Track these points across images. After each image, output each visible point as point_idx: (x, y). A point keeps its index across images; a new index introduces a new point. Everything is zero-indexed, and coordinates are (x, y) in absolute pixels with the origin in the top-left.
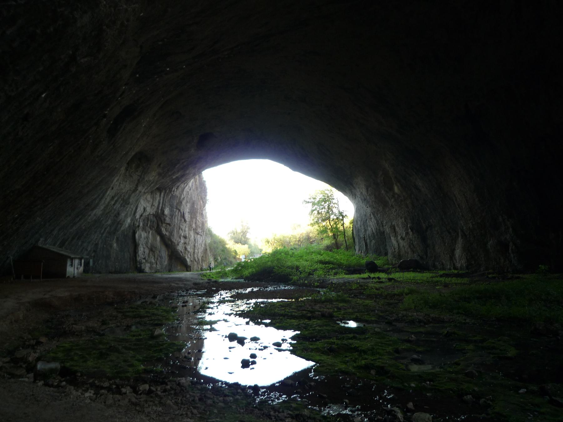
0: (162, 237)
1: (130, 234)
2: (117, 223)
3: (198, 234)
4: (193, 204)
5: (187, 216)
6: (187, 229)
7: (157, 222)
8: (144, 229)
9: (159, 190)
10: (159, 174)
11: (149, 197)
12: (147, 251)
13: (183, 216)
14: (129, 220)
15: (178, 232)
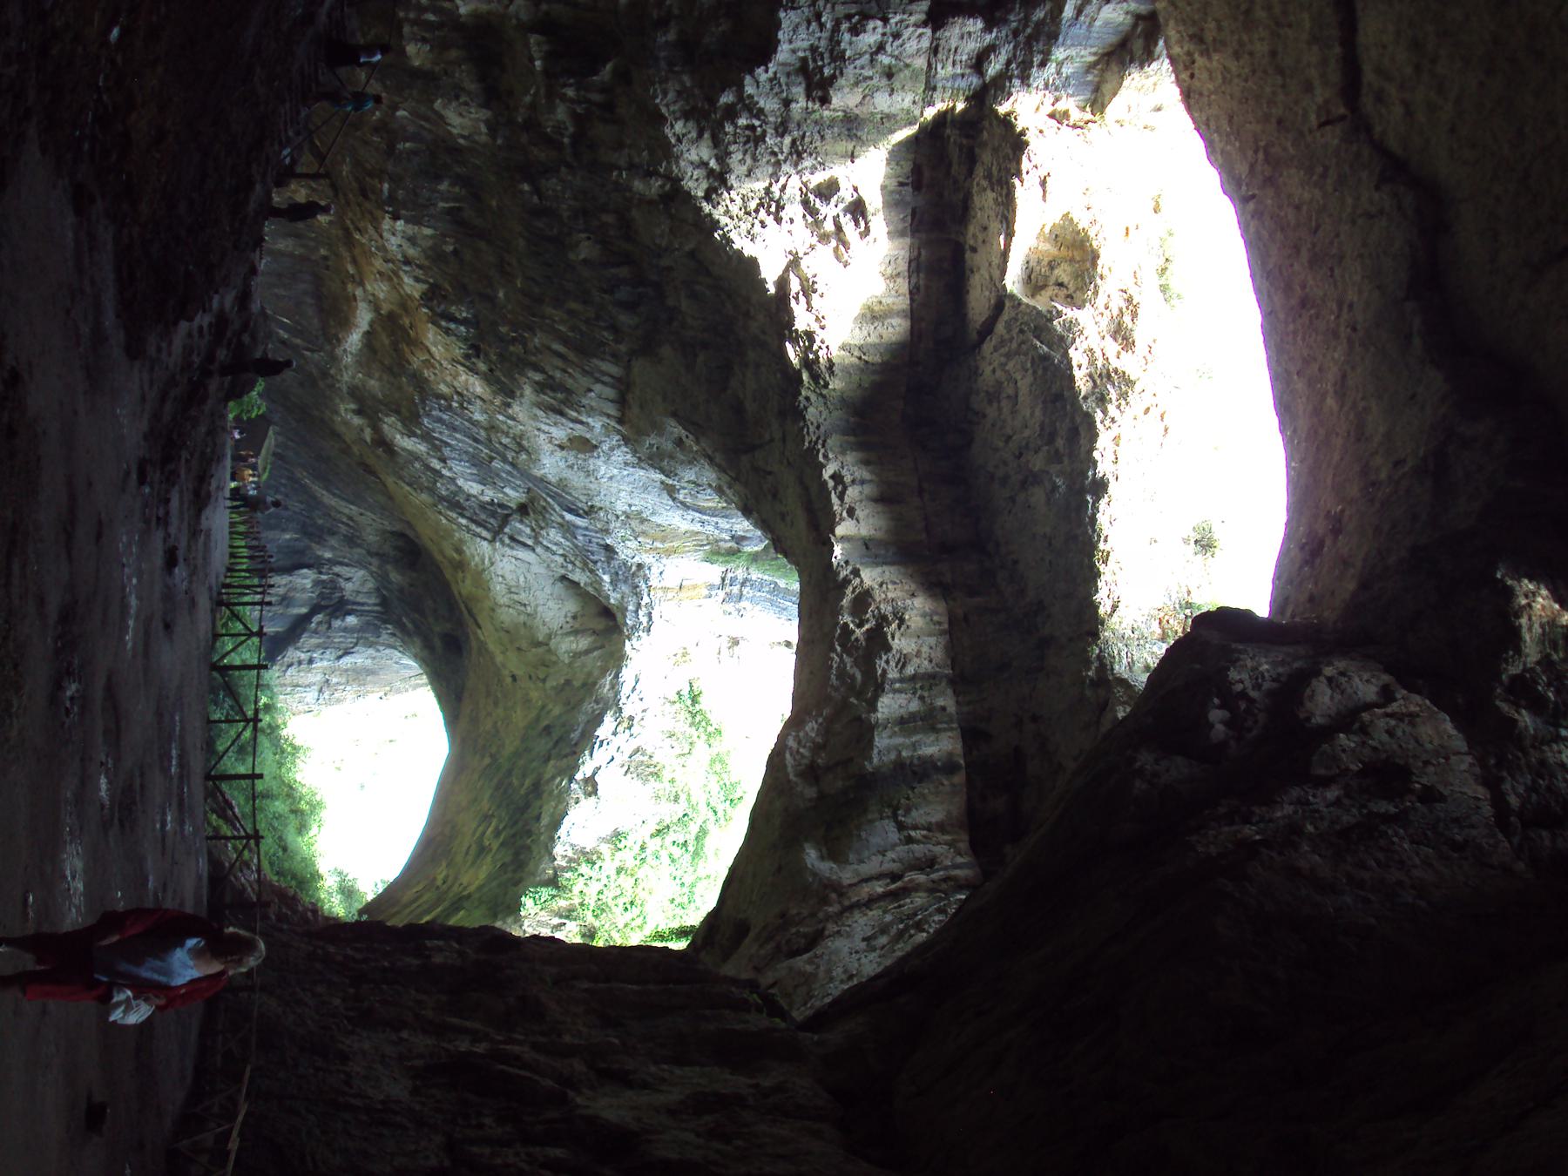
0: (306, 618)
1: (306, 560)
2: (317, 534)
3: (320, 691)
4: (370, 672)
5: (347, 661)
6: (325, 663)
7: (332, 605)
8: (316, 583)
9: (384, 602)
10: (401, 590)
11: (370, 585)
12: (282, 591)
13: (347, 653)
14: (328, 555)
15: (318, 646)
